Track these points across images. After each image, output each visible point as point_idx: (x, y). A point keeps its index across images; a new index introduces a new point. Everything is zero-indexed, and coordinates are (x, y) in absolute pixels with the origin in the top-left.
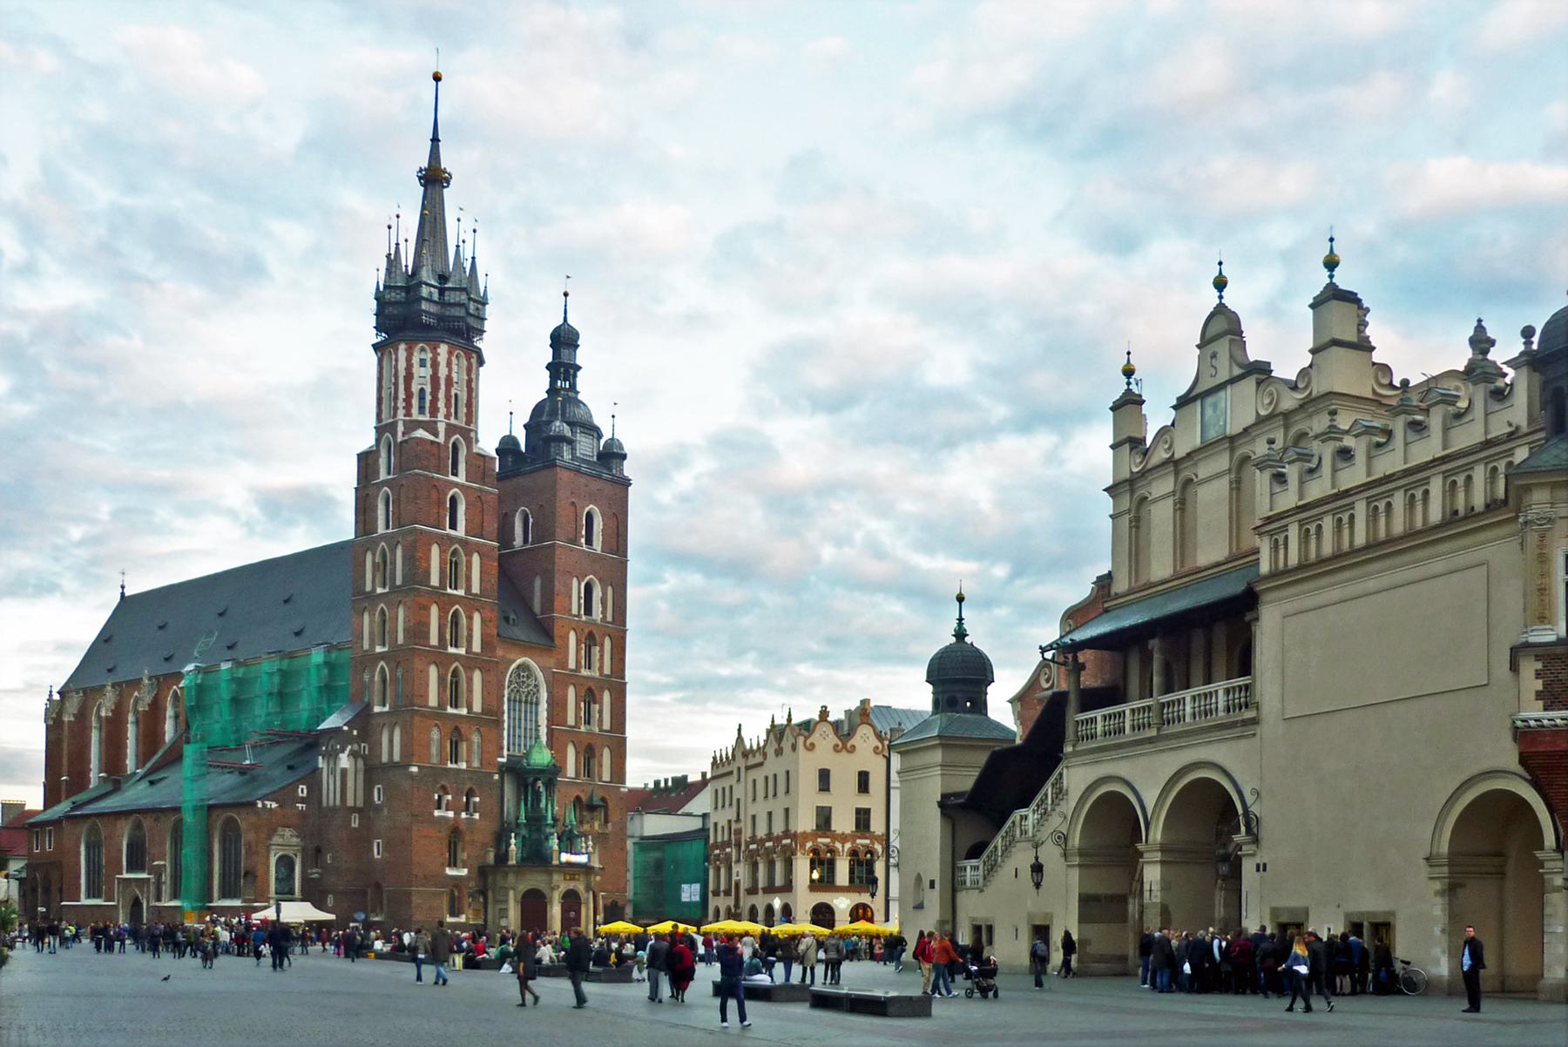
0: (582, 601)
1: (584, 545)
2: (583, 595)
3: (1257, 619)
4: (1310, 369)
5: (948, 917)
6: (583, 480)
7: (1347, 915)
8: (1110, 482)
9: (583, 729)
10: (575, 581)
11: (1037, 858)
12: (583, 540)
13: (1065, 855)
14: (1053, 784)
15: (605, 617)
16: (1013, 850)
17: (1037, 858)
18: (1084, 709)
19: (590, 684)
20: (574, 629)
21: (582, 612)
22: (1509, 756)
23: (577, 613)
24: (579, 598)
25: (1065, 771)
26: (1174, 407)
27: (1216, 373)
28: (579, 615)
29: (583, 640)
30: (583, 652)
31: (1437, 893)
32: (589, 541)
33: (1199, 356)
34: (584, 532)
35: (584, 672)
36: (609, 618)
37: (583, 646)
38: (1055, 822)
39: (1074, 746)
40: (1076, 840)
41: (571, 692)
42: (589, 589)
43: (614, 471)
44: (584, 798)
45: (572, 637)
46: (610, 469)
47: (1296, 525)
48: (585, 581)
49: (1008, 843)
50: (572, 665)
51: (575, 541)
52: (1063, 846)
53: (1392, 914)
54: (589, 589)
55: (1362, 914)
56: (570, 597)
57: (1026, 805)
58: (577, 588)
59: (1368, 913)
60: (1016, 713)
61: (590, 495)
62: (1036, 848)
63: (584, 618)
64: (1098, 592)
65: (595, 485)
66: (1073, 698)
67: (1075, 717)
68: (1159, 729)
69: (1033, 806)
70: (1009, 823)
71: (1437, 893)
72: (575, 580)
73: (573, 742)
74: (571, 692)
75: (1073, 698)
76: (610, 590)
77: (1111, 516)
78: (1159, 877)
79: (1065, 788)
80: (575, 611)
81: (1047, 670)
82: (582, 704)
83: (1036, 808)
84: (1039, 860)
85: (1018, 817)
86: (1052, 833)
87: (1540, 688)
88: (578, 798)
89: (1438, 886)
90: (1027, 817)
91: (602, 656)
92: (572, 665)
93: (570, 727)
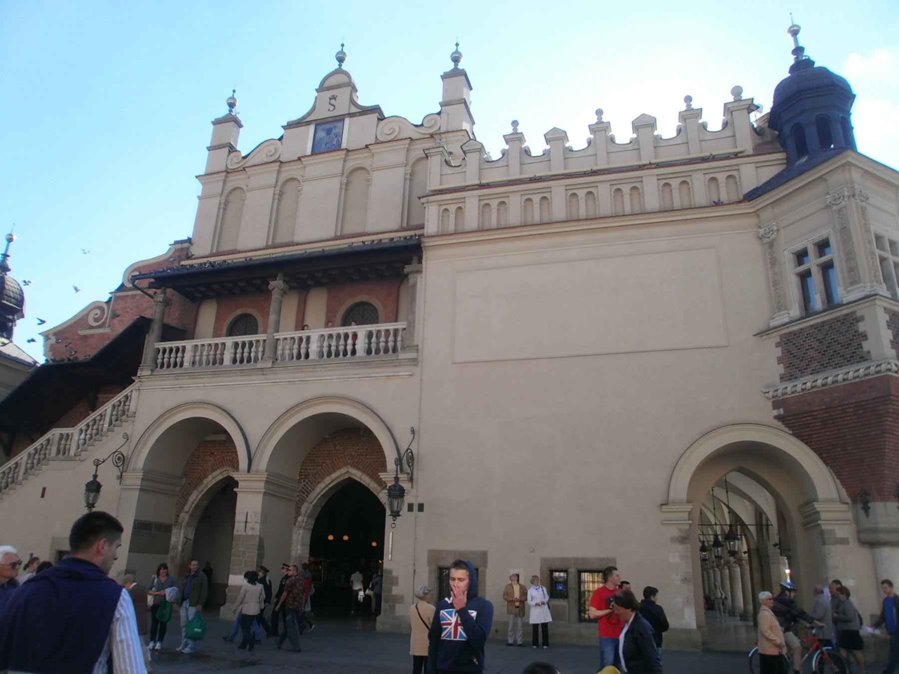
3: (420, 271)
4: (438, 117)
7: (544, 561)
8: (202, 172)
11: (95, 476)
13: (121, 477)
14: (114, 406)
16: (44, 468)
17: (95, 476)
18: (163, 339)
22: (769, 414)
25: (135, 394)
26: (284, 127)
27: (334, 110)
31: (674, 540)
33: (316, 97)
38: (113, 443)
39: (152, 370)
47: (476, 200)
49: (35, 461)
52: (121, 468)
55: (568, 559)
59: (576, 559)
60: (49, 346)
62: (97, 466)
64: (174, 253)
66: (156, 329)
67: (153, 344)
68: (273, 362)
69: (82, 425)
70: (43, 440)
71: (674, 540)
75: (156, 329)
77: (198, 197)
78: (259, 509)
79: (132, 409)
81: (98, 312)
83: (84, 428)
84: (98, 480)
85: (57, 437)
86: (114, 453)
87: (864, 344)
89: (675, 532)
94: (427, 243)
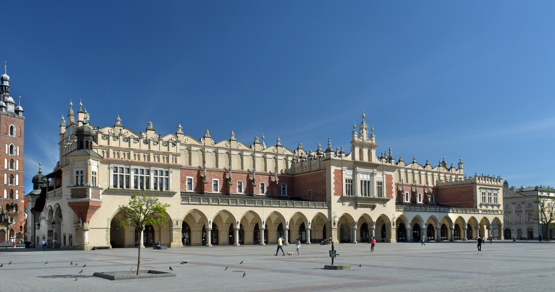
0: (9, 150)
1: (10, 135)
2: (9, 149)
5: (33, 235)
6: (9, 117)
9: (9, 185)
10: (7, 145)
12: (9, 134)
15: (16, 154)
18: (49, 191)
19: (11, 173)
20: (6, 158)
21: (9, 153)
23: (7, 154)
24: (8, 149)
28: (8, 154)
29: (10, 161)
30: (9, 164)
32: (11, 134)
34: (10, 132)
35: (10, 169)
36: (18, 154)
37: (9, 162)
40: (47, 219)
41: (6, 175)
42: (11, 147)
43: (19, 115)
44: (10, 204)
45: (6, 160)
46: (18, 114)
48: (10, 145)
50: (6, 167)
51: (7, 134)
53: (72, 234)
54: (11, 147)
56: (5, 149)
57: (42, 211)
58: (7, 147)
61: (12, 122)
63: (10, 155)
65: (13, 119)
72: (7, 145)
73: (6, 189)
74: (6, 175)
76: (18, 147)
80: (7, 153)
82: (9, 179)
88: (8, 204)
90: (43, 214)
91: (16, 165)
92: (6, 167)
93: (5, 184)
94: (62, 169)
